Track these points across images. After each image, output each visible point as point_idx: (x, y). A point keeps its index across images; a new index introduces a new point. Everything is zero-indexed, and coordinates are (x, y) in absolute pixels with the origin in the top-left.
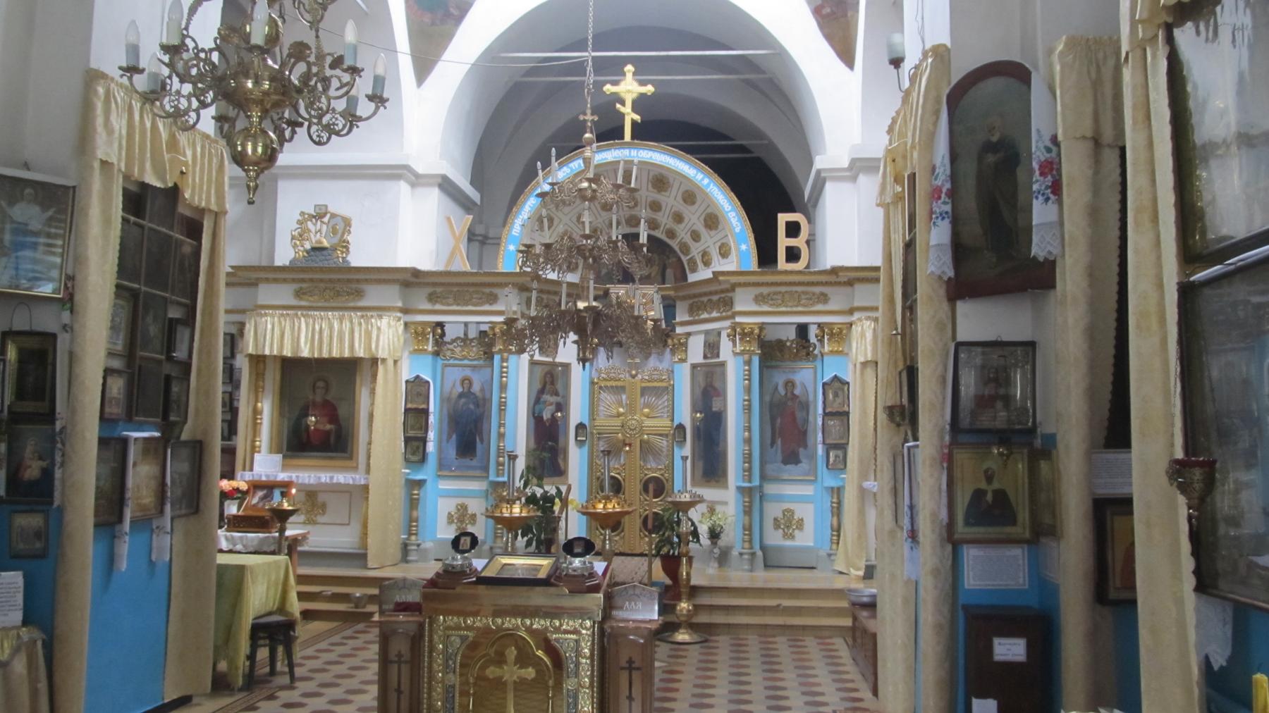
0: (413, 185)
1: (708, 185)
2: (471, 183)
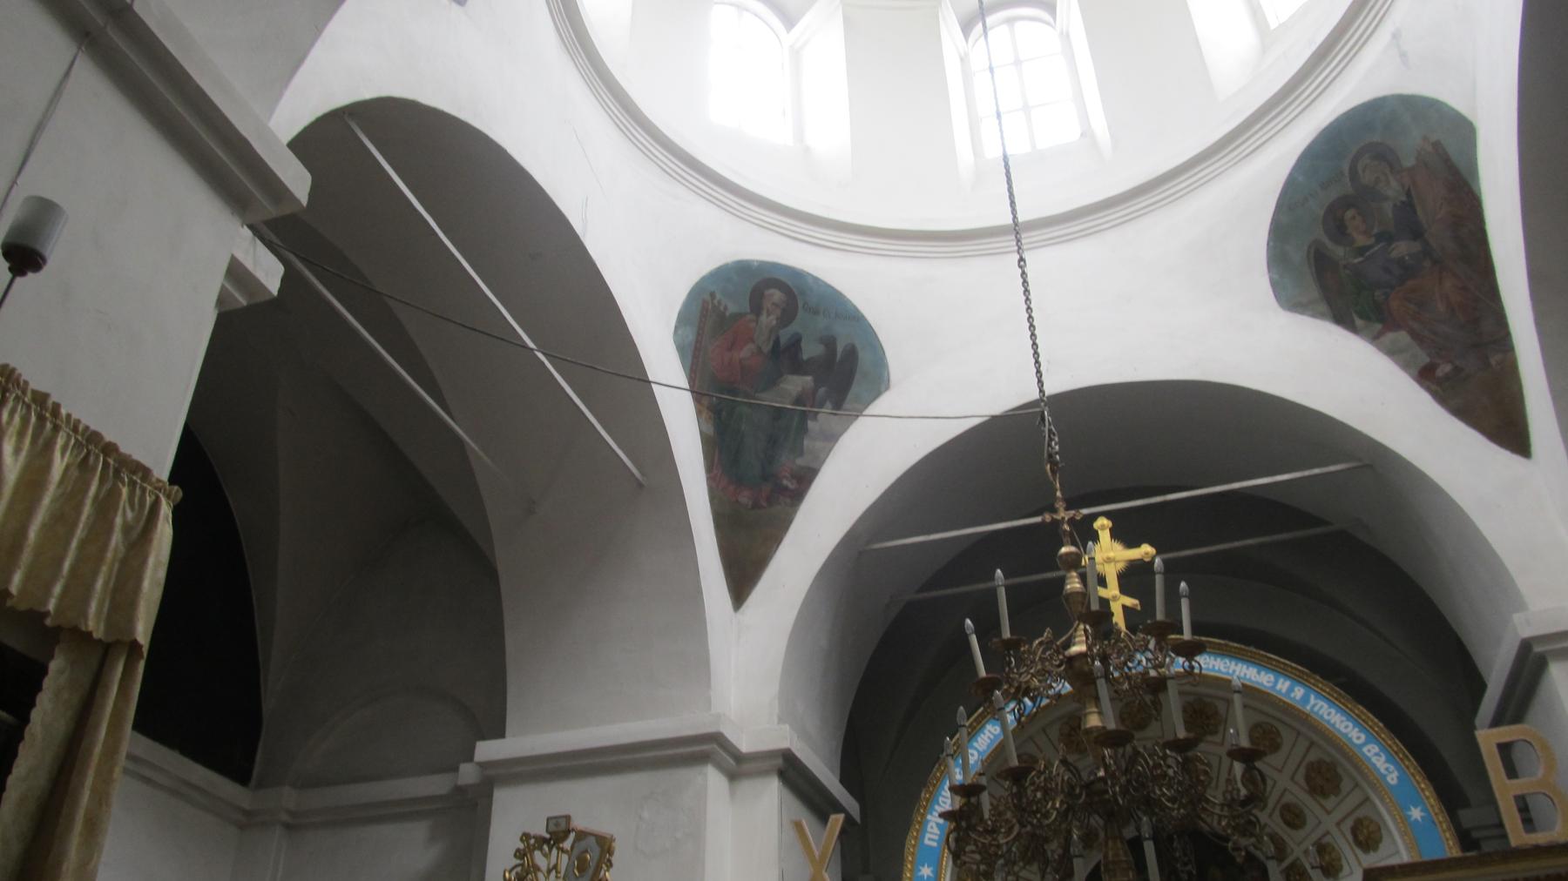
0: (733, 777)
1: (1305, 699)
2: (844, 780)
